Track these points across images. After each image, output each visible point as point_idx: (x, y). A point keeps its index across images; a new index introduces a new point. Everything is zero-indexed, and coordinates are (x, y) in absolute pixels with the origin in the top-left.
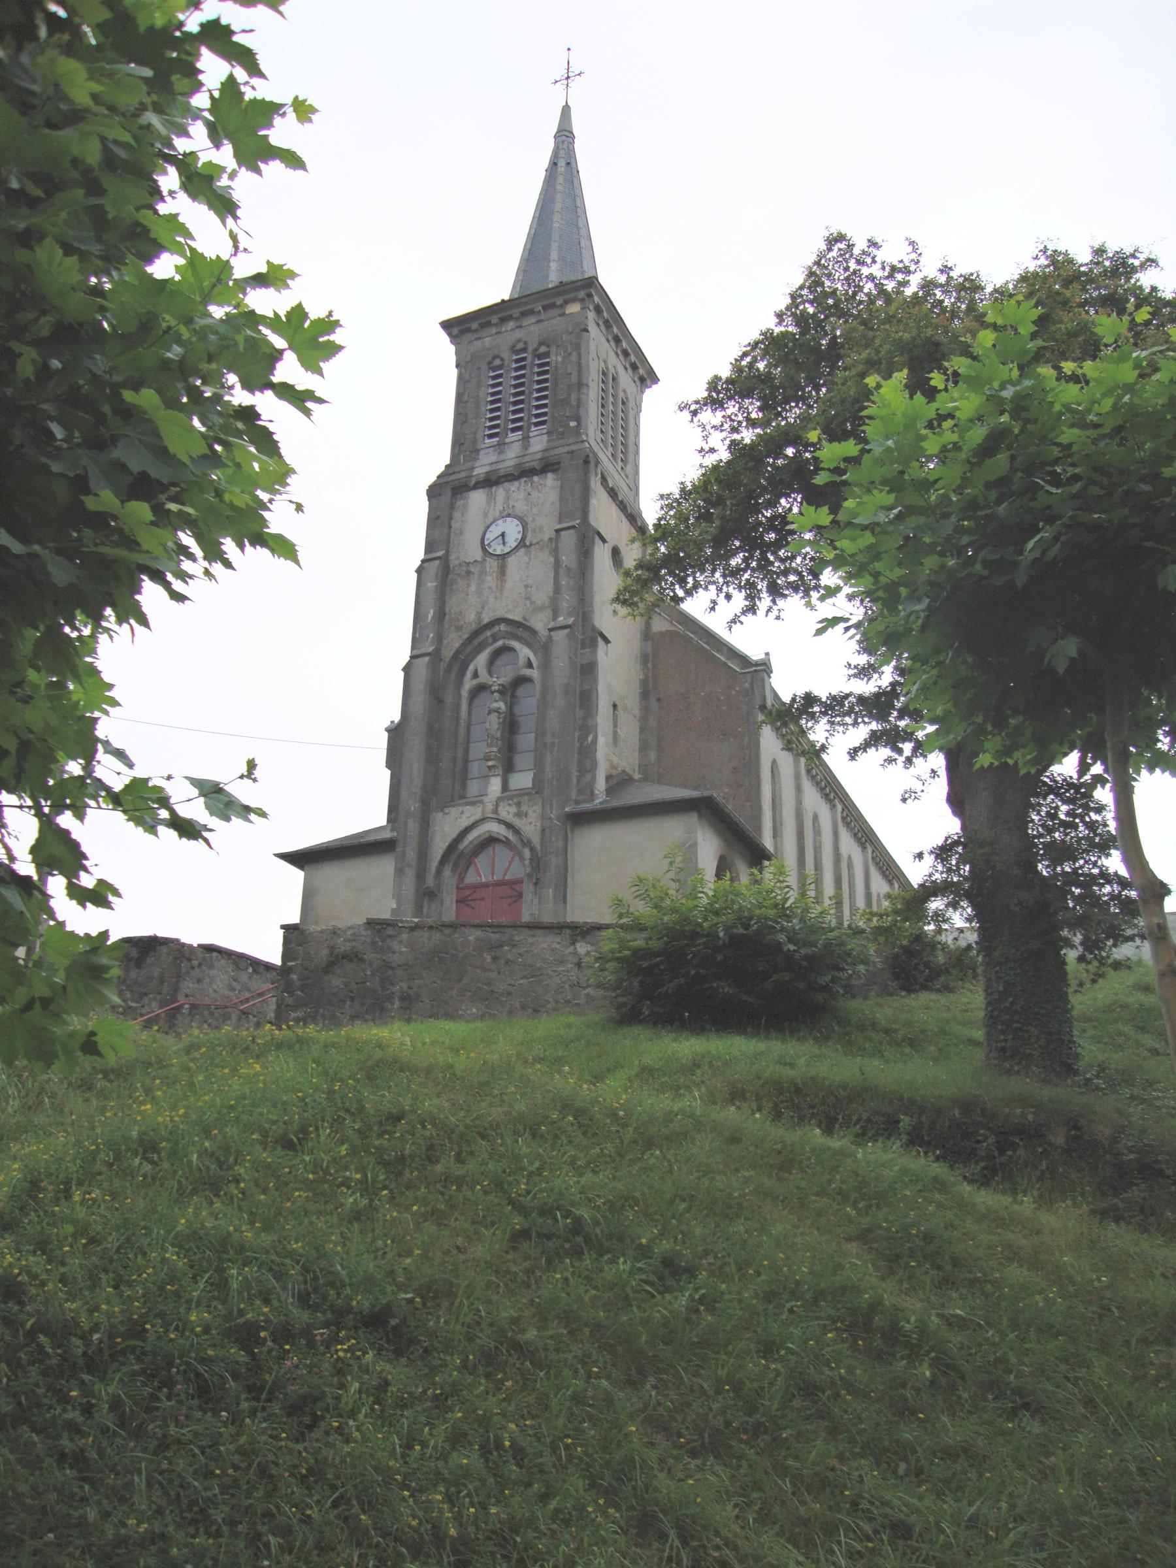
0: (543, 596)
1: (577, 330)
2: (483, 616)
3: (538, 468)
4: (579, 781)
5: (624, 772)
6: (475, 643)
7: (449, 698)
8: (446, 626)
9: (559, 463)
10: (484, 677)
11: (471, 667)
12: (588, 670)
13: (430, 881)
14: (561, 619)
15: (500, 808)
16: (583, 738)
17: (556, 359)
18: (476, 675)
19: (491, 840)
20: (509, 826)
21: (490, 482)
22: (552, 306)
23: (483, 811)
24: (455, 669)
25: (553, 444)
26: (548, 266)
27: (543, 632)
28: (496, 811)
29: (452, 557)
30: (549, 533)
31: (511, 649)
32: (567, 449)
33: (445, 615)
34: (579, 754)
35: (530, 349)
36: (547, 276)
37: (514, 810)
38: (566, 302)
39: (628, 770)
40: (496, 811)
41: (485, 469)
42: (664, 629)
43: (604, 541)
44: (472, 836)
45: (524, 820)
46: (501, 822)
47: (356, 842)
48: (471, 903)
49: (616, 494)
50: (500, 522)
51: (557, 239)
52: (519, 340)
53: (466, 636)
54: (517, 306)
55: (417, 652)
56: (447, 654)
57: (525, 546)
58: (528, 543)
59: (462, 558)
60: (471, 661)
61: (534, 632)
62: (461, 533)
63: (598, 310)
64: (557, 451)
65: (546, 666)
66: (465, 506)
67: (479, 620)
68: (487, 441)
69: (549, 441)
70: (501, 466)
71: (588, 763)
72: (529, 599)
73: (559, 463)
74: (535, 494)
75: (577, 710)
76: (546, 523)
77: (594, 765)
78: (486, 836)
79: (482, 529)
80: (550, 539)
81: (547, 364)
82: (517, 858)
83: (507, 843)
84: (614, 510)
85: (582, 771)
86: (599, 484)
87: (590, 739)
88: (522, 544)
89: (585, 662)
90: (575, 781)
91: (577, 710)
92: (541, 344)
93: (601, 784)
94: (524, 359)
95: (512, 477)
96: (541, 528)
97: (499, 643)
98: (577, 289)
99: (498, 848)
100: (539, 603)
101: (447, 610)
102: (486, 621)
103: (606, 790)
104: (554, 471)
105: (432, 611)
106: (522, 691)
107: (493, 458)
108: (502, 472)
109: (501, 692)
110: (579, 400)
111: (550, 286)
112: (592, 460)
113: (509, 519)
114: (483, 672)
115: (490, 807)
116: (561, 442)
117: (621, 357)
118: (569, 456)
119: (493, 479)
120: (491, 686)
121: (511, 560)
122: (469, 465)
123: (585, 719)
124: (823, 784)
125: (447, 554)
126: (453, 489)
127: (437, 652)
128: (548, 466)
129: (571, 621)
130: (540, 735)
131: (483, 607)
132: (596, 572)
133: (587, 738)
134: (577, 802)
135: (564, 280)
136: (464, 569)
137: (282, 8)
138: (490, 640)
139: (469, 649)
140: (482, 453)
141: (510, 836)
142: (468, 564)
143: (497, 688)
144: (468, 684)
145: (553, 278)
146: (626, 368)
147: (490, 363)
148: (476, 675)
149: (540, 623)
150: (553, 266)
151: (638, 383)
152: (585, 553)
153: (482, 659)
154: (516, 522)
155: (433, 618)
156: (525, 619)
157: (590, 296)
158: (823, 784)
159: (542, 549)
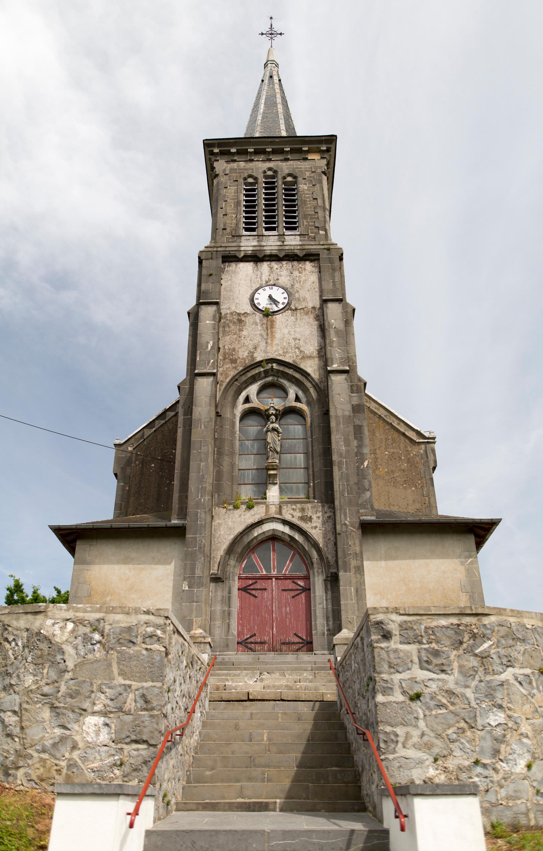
2: (255, 355)
6: (249, 374)
17: (303, 187)
18: (247, 400)
20: (292, 526)
22: (300, 151)
28: (280, 513)
35: (280, 176)
37: (298, 514)
44: (257, 532)
46: (285, 522)
48: (253, 592)
52: (270, 169)
57: (291, 310)
59: (233, 308)
62: (231, 291)
66: (235, 272)
67: (253, 358)
74: (296, 273)
78: (271, 533)
88: (287, 307)
92: (290, 175)
97: (270, 379)
102: (259, 359)
104: (311, 261)
105: (211, 343)
108: (268, 252)
119: (261, 256)
121: (278, 318)
126: (223, 257)
131: (255, 348)
133: (363, 464)
136: (236, 317)
138: (263, 375)
139: (244, 378)
140: (243, 238)
141: (297, 536)
142: (239, 314)
143: (274, 412)
144: (241, 407)
147: (245, 179)
148: (247, 400)
153: (253, 389)
159: (307, 314)
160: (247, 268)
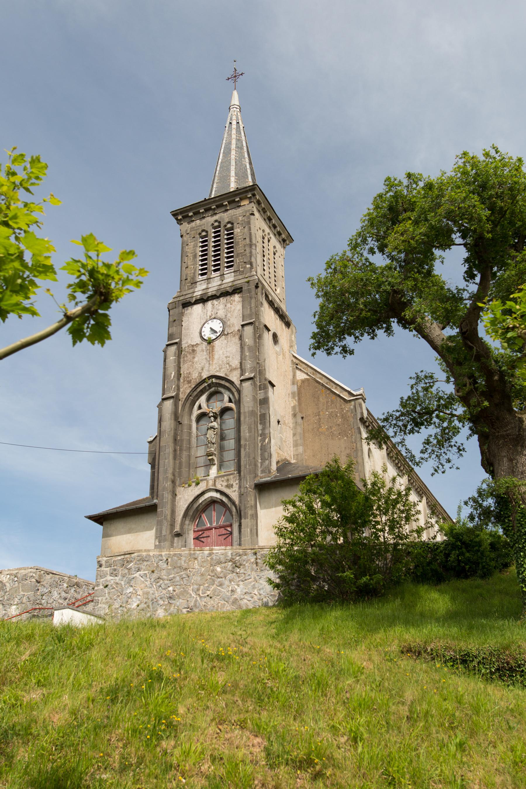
0: (236, 363)
1: (248, 214)
2: (202, 374)
3: (230, 291)
4: (261, 465)
5: (286, 459)
6: (199, 390)
7: (185, 421)
8: (182, 380)
9: (242, 288)
10: (205, 408)
11: (197, 404)
12: (265, 402)
13: (177, 529)
14: (247, 374)
15: (217, 483)
16: (263, 440)
17: (237, 231)
18: (200, 407)
19: (213, 502)
20: (222, 493)
21: (203, 300)
22: (234, 201)
23: (207, 485)
24: (188, 405)
25: (237, 278)
26: (230, 179)
27: (237, 382)
28: (215, 485)
29: (183, 343)
30: (238, 327)
31: (220, 393)
32: (246, 280)
33: (181, 374)
34: (261, 449)
35: (222, 226)
36: (229, 185)
37: (225, 484)
38: (241, 199)
39: (288, 458)
40: (215, 485)
41: (200, 293)
42: (303, 378)
43: (268, 330)
44: (201, 500)
45: (232, 489)
46: (217, 491)
47: (134, 507)
48: (202, 539)
49: (273, 304)
50: (210, 322)
51: (234, 164)
52: (216, 221)
53: (193, 386)
54: (214, 202)
55: (164, 396)
56: (183, 396)
57: (225, 335)
58: (226, 333)
59: (190, 342)
60: (198, 399)
61: (231, 382)
62: (188, 329)
63: (259, 203)
64: (239, 282)
65: (238, 403)
66: (191, 314)
67: (201, 376)
68: (200, 277)
69: (234, 276)
70: (210, 290)
71: (266, 454)
72: (228, 364)
73: (242, 288)
74: (229, 305)
75: (259, 425)
76: (236, 322)
77: (270, 456)
78: (210, 499)
79: (200, 326)
80: (239, 330)
81: (232, 233)
82: (228, 511)
83: (222, 503)
84: (272, 312)
85: (263, 459)
86: (264, 299)
87: (267, 441)
88: (223, 333)
89: (262, 397)
90: (259, 465)
91: (259, 425)
92: (229, 222)
93: (274, 467)
94: (219, 231)
95: (214, 297)
96: (233, 325)
97: (213, 389)
98: (247, 192)
99: (217, 506)
100: (234, 366)
101: (182, 372)
102: (204, 377)
103: (277, 469)
104: (239, 293)
105: (173, 373)
106: (226, 416)
107: (204, 287)
108: (210, 294)
109: (215, 418)
110: (251, 252)
111: (231, 190)
112: (260, 285)
113: (215, 320)
114: (204, 405)
115: (211, 483)
116: (240, 277)
117: (273, 229)
118: (246, 284)
119: (205, 298)
120: (209, 414)
121: (217, 343)
122: (191, 291)
123: (263, 429)
124: (419, 490)
125: (181, 341)
126: (183, 304)
127: (177, 395)
128: (237, 290)
129: (252, 375)
130: (238, 440)
131: (202, 369)
132: (266, 348)
133: (265, 441)
134: (261, 478)
135: (239, 187)
136: (191, 348)
137: (226, 450)
138: (207, 388)
139: (195, 393)
140: (198, 283)
141: (224, 499)
142: (193, 346)
143: (212, 414)
144: (196, 412)
145: (233, 186)
146: (275, 235)
147: (200, 234)
148: (200, 407)
149: (235, 377)
150: (233, 179)
151: (282, 243)
152: (258, 338)
153: (203, 398)
154: (219, 321)
155: (174, 376)
156: (226, 375)
157: (254, 195)
158: (419, 490)
159: (234, 336)
160: (198, 308)
